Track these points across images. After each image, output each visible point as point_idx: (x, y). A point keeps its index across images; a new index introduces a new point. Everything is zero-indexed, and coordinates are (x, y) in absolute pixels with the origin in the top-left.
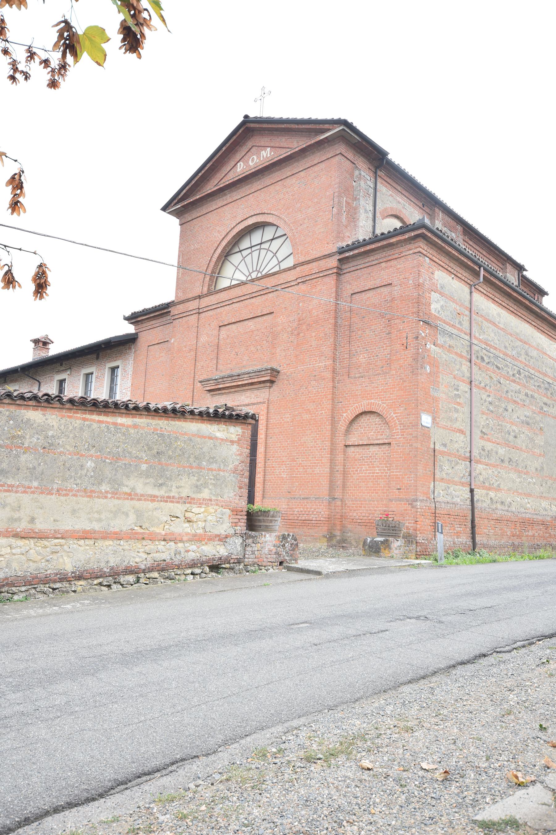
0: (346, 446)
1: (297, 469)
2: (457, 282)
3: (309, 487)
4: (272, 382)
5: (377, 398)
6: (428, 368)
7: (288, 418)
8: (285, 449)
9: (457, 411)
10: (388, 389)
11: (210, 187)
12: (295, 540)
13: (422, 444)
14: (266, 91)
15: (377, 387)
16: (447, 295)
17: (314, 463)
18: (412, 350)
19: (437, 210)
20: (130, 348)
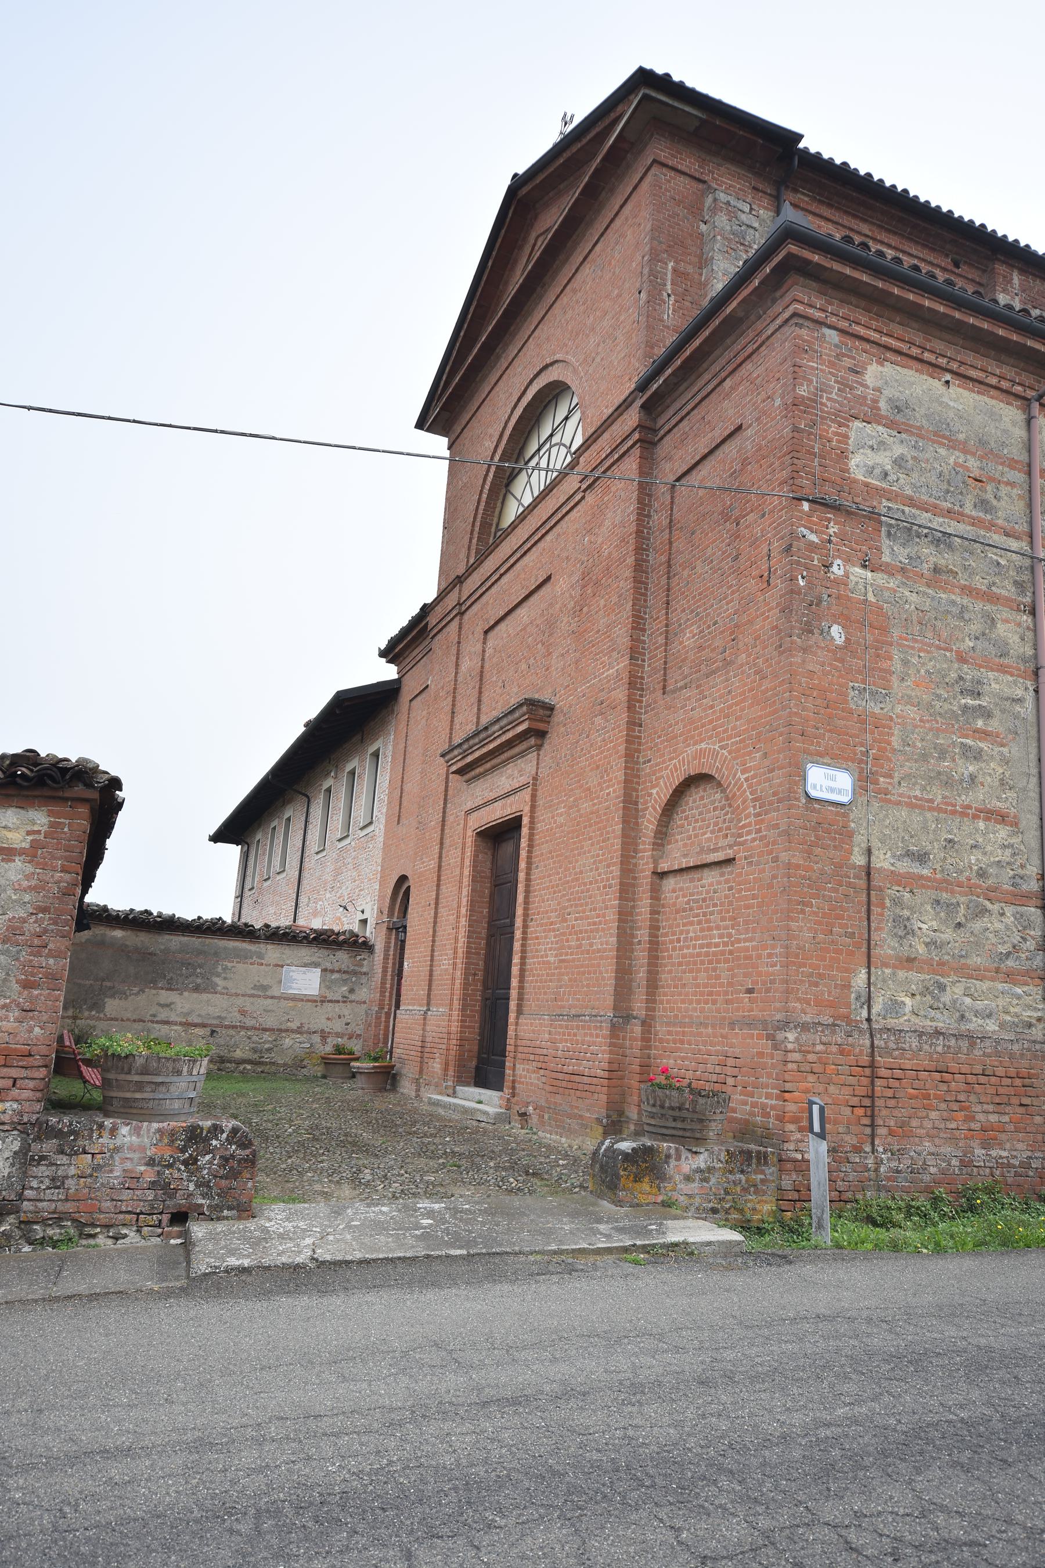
0: (663, 875)
2: (966, 393)
4: (542, 734)
5: (710, 738)
6: (836, 632)
9: (978, 756)
10: (730, 707)
12: (242, 1146)
13: (810, 853)
14: (568, 119)
15: (712, 707)
16: (920, 428)
18: (780, 585)
19: (1001, 268)
20: (393, 711)
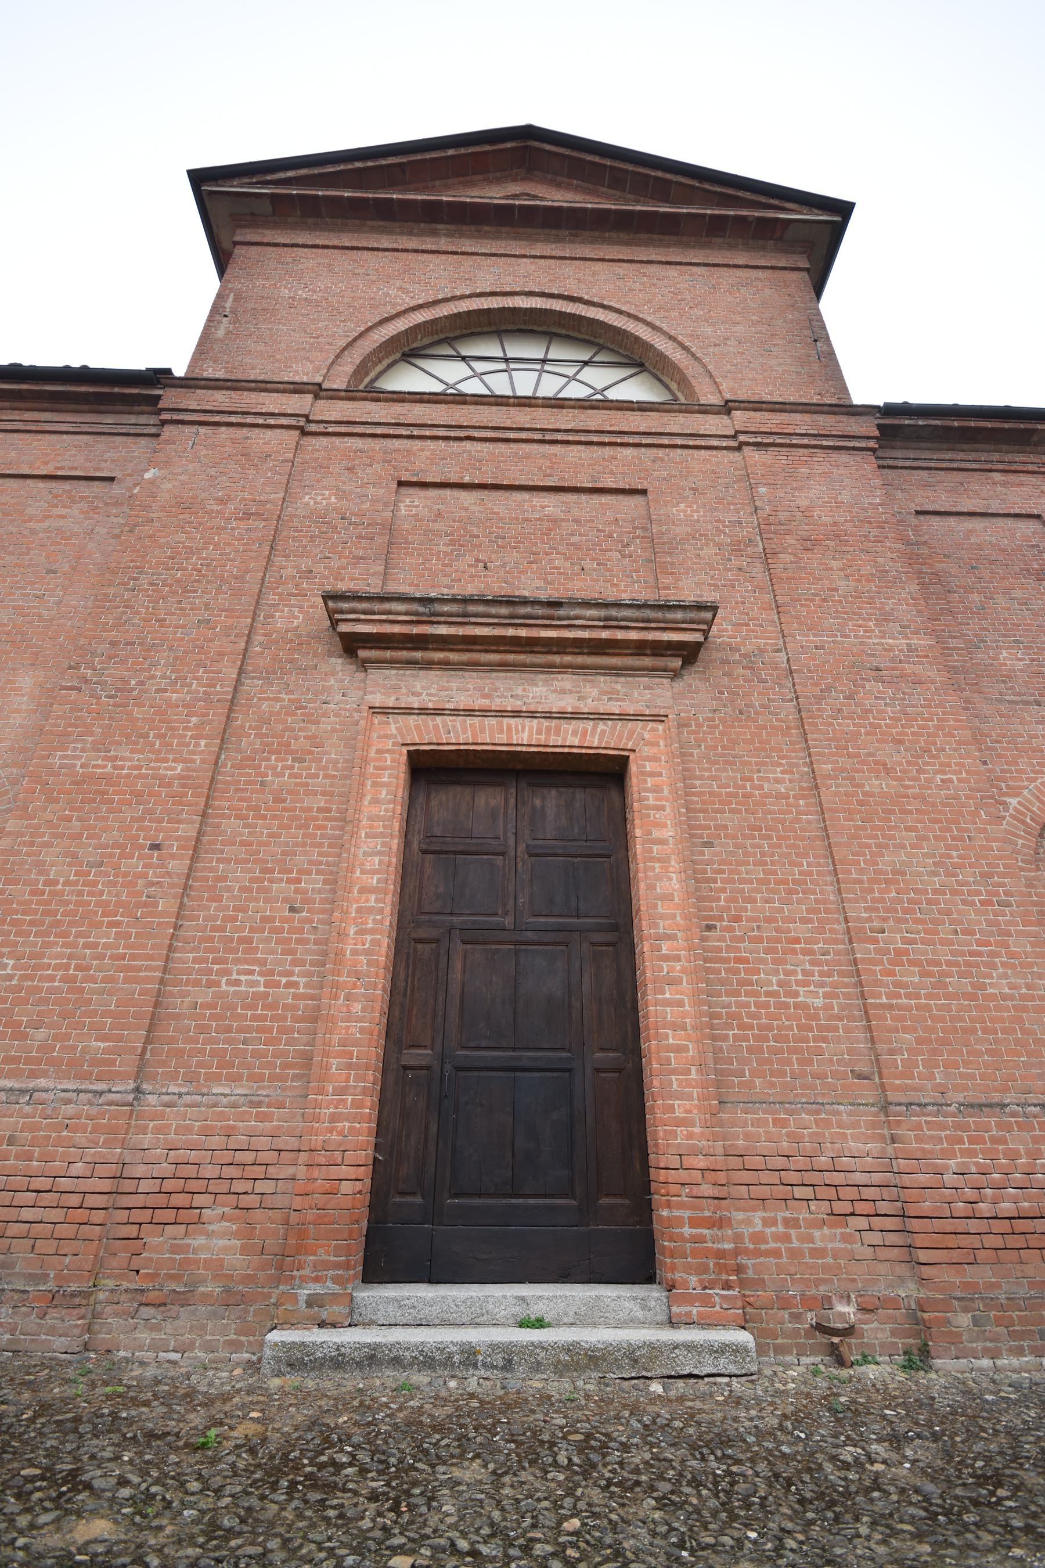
1: (892, 973)
3: (979, 1054)
7: (777, 781)
8: (790, 892)
17: (972, 954)
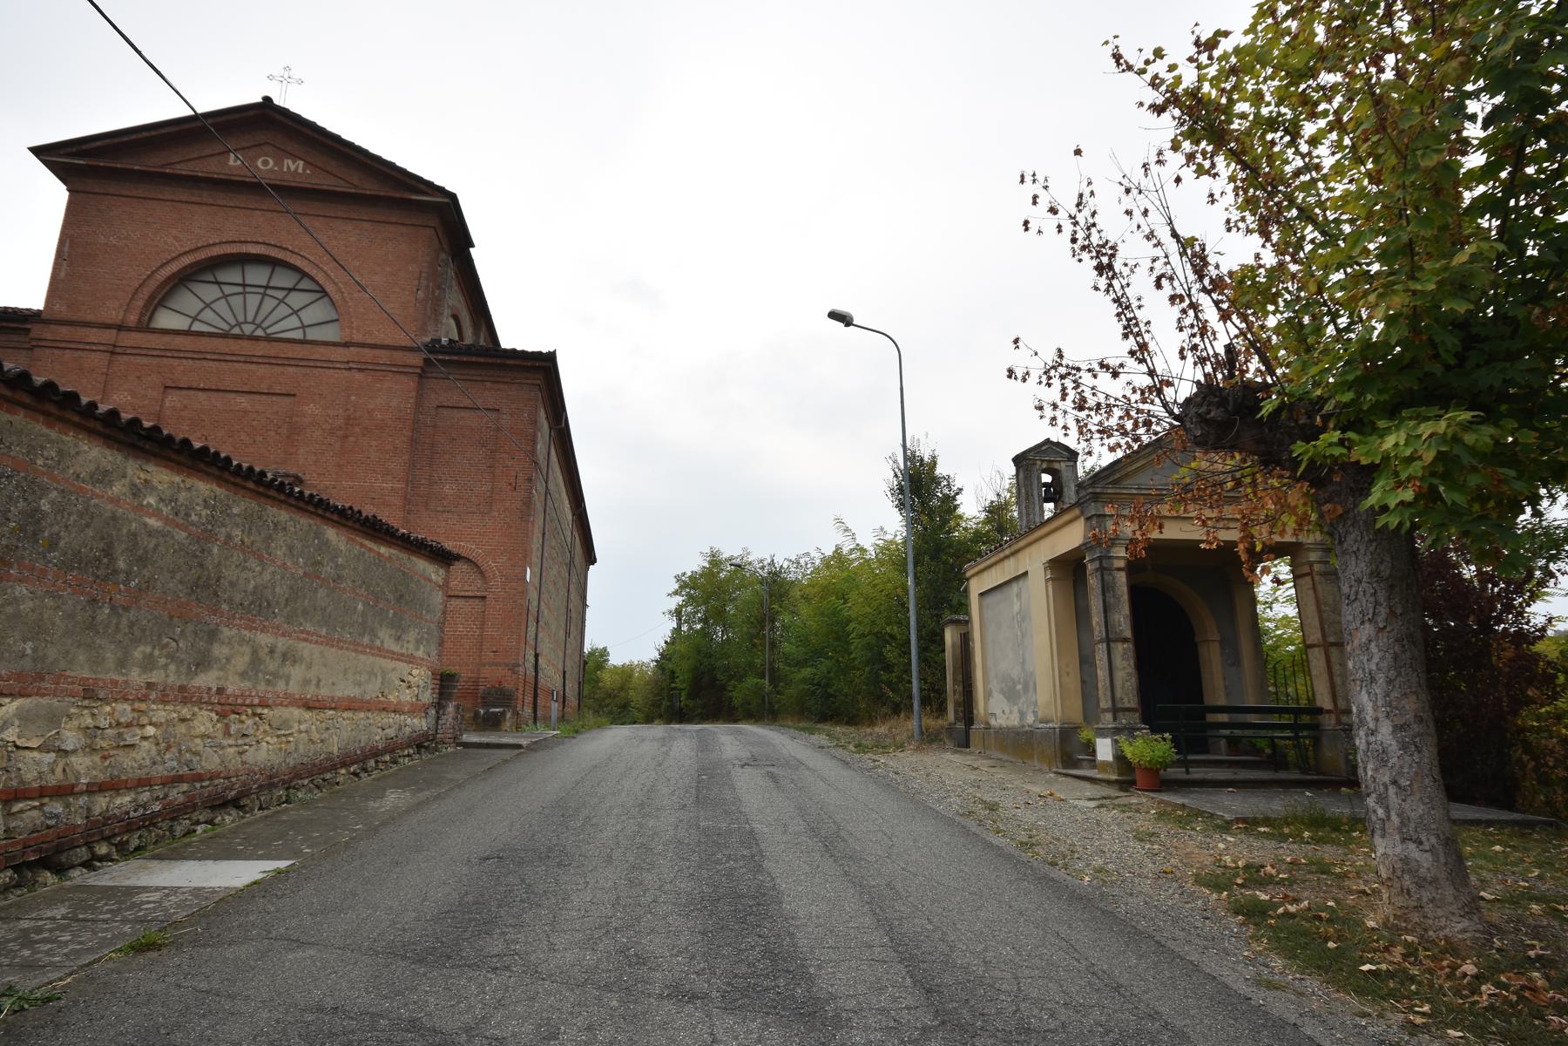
11: (152, 162)
